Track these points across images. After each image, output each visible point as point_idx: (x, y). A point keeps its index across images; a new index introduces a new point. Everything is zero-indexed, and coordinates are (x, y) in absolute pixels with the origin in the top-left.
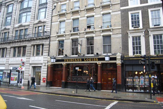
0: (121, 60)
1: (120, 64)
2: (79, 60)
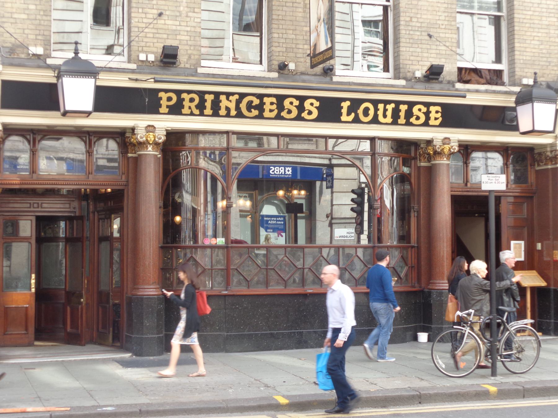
2: (301, 108)
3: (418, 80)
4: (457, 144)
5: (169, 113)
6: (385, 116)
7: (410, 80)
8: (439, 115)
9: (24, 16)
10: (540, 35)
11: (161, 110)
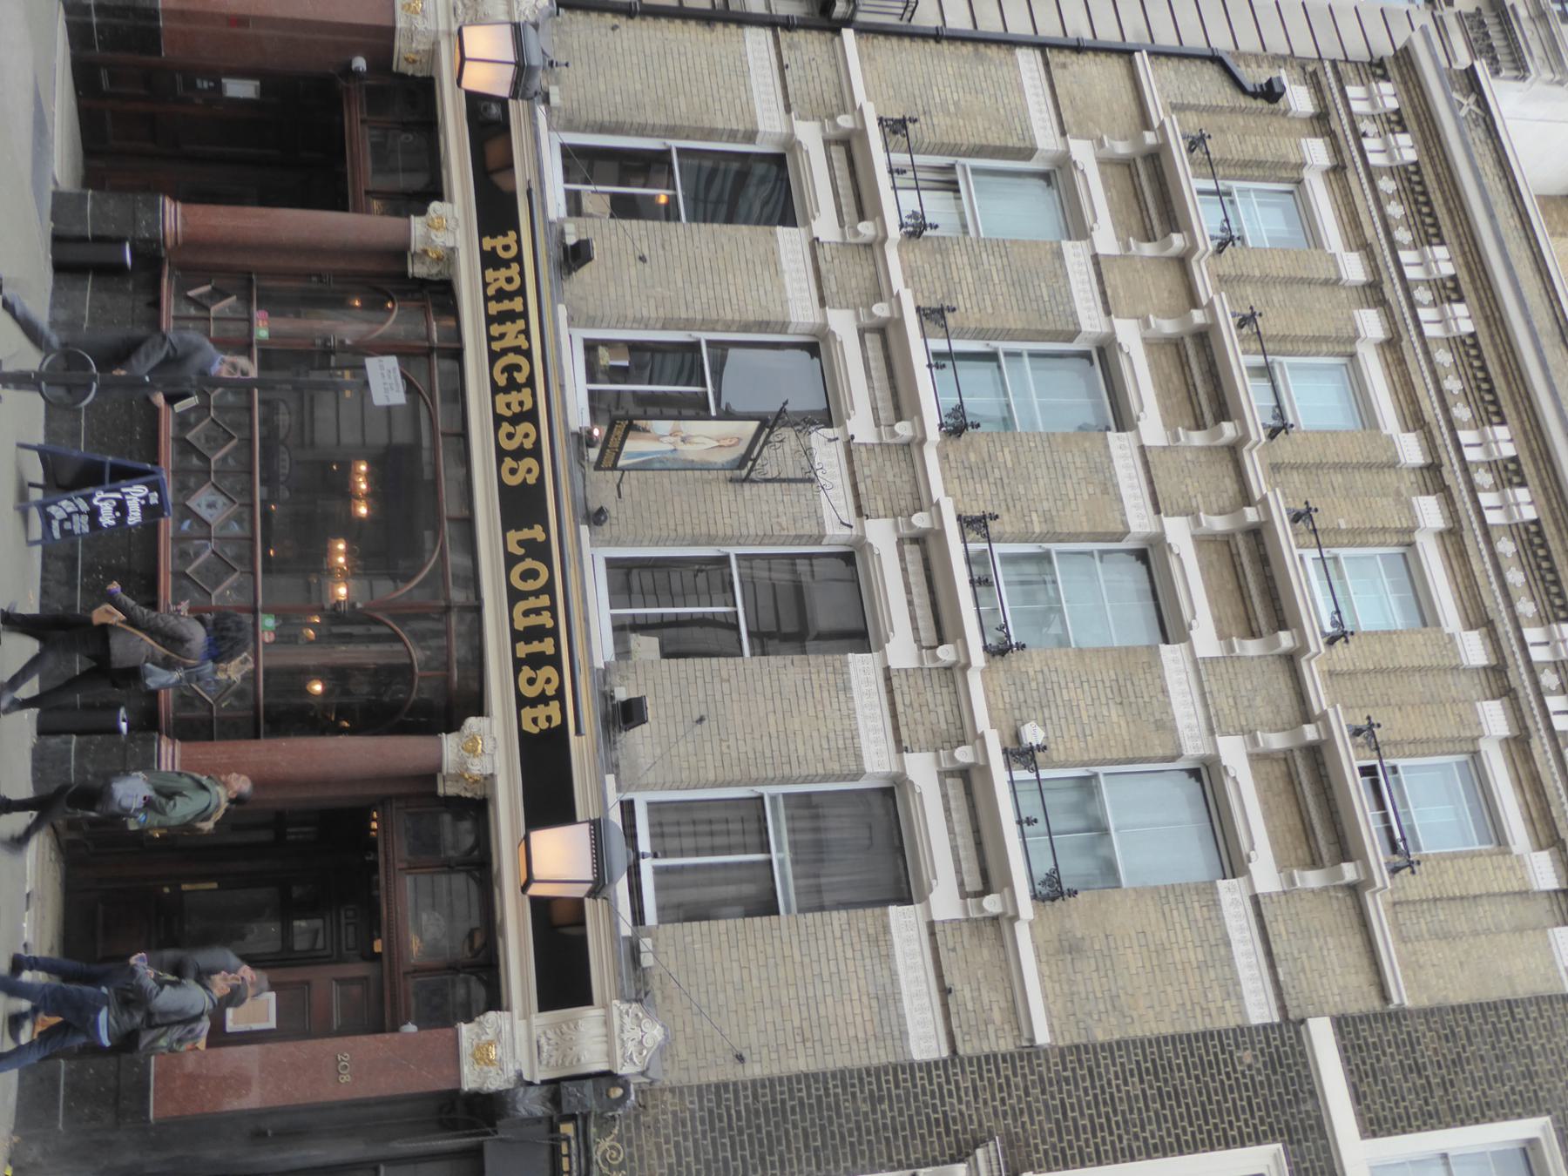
0: (555, 1088)
2: (519, 454)
3: (607, 697)
6: (526, 613)
8: (544, 725)
10: (755, 983)
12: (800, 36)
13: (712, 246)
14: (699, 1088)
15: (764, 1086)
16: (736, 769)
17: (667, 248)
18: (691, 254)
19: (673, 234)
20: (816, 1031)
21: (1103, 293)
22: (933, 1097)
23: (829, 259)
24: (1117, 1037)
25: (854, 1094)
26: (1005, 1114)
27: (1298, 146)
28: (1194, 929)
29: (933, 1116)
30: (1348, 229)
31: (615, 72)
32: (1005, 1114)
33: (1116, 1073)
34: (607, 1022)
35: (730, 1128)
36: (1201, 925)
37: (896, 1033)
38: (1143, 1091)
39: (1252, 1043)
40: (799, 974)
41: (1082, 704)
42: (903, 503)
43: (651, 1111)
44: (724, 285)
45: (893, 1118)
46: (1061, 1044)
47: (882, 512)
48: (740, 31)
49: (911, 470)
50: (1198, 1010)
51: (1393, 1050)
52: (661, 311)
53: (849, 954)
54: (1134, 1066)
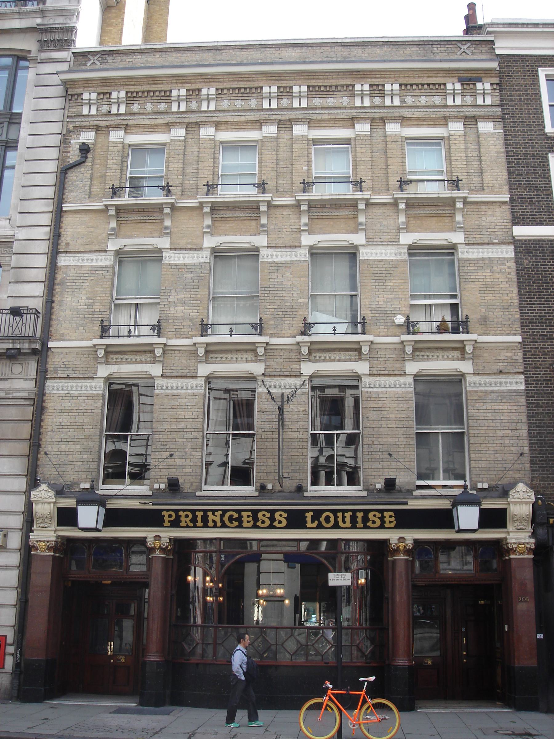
1: (530, 550)
2: (272, 519)
3: (380, 491)
4: (412, 542)
5: (171, 526)
6: (344, 522)
7: (373, 492)
8: (393, 519)
9: (80, 463)
10: (495, 445)
11: (165, 524)
12: (50, 367)
13: (164, 423)
14: (532, 471)
15: (532, 447)
16: (411, 443)
17: (165, 443)
18: (169, 433)
19: (158, 440)
20: (513, 424)
21: (190, 249)
22: (538, 384)
23: (171, 371)
24: (518, 310)
25: (536, 413)
26: (544, 358)
27: (114, 143)
28: (478, 271)
29: (545, 385)
30: (157, 130)
31: (71, 456)
32: (544, 358)
33: (531, 313)
34: (515, 503)
35: (546, 461)
36: (476, 268)
37: (515, 394)
38: (538, 304)
39: (521, 258)
40: (491, 428)
41: (385, 296)
42: (294, 357)
43: (539, 489)
44: (185, 420)
45: (545, 400)
46: (520, 332)
47: (298, 367)
48: (47, 395)
49: (278, 350)
50: (509, 276)
51: (524, 205)
52: (198, 450)
53: (485, 408)
54: (529, 306)
